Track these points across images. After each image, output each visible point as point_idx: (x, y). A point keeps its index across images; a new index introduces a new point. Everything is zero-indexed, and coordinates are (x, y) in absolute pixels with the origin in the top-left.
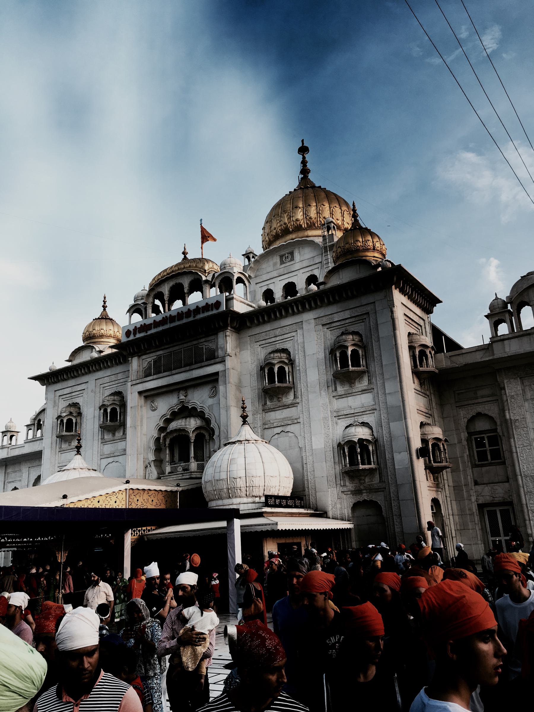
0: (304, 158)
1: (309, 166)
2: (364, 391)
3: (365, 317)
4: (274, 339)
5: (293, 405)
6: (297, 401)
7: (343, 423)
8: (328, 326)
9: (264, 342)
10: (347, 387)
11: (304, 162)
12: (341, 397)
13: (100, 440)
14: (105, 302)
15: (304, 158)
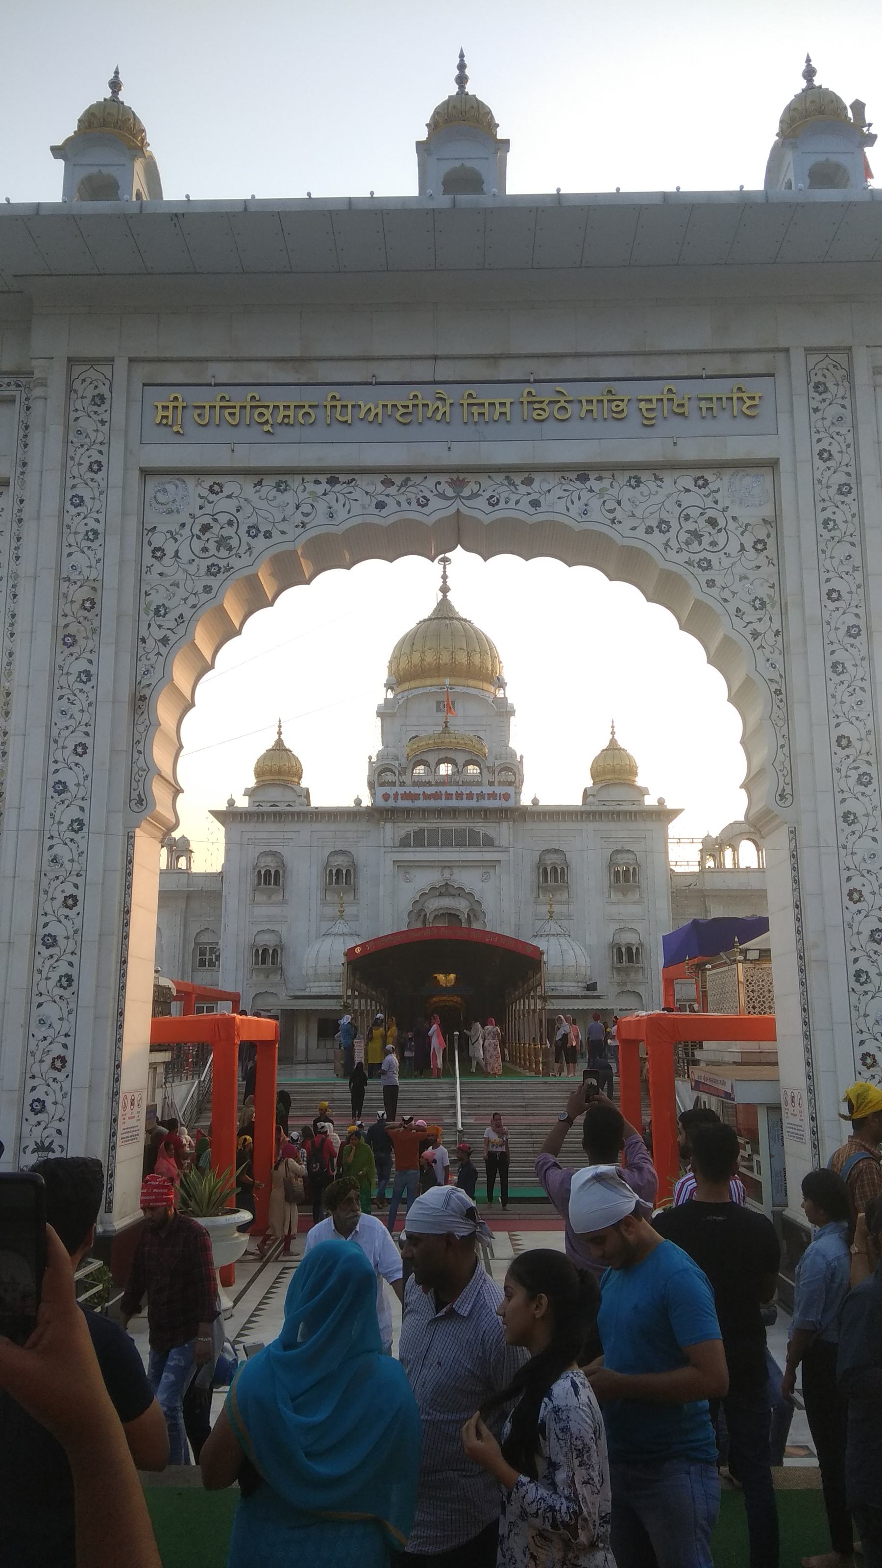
0: (445, 572)
1: (449, 583)
2: (634, 903)
3: (641, 840)
4: (551, 839)
5: (567, 903)
6: (571, 900)
7: (614, 927)
8: (605, 839)
9: (539, 839)
10: (620, 896)
11: (445, 577)
12: (613, 903)
13: (319, 901)
14: (280, 727)
15: (445, 572)
